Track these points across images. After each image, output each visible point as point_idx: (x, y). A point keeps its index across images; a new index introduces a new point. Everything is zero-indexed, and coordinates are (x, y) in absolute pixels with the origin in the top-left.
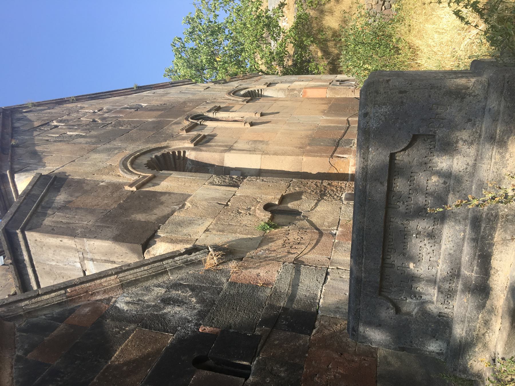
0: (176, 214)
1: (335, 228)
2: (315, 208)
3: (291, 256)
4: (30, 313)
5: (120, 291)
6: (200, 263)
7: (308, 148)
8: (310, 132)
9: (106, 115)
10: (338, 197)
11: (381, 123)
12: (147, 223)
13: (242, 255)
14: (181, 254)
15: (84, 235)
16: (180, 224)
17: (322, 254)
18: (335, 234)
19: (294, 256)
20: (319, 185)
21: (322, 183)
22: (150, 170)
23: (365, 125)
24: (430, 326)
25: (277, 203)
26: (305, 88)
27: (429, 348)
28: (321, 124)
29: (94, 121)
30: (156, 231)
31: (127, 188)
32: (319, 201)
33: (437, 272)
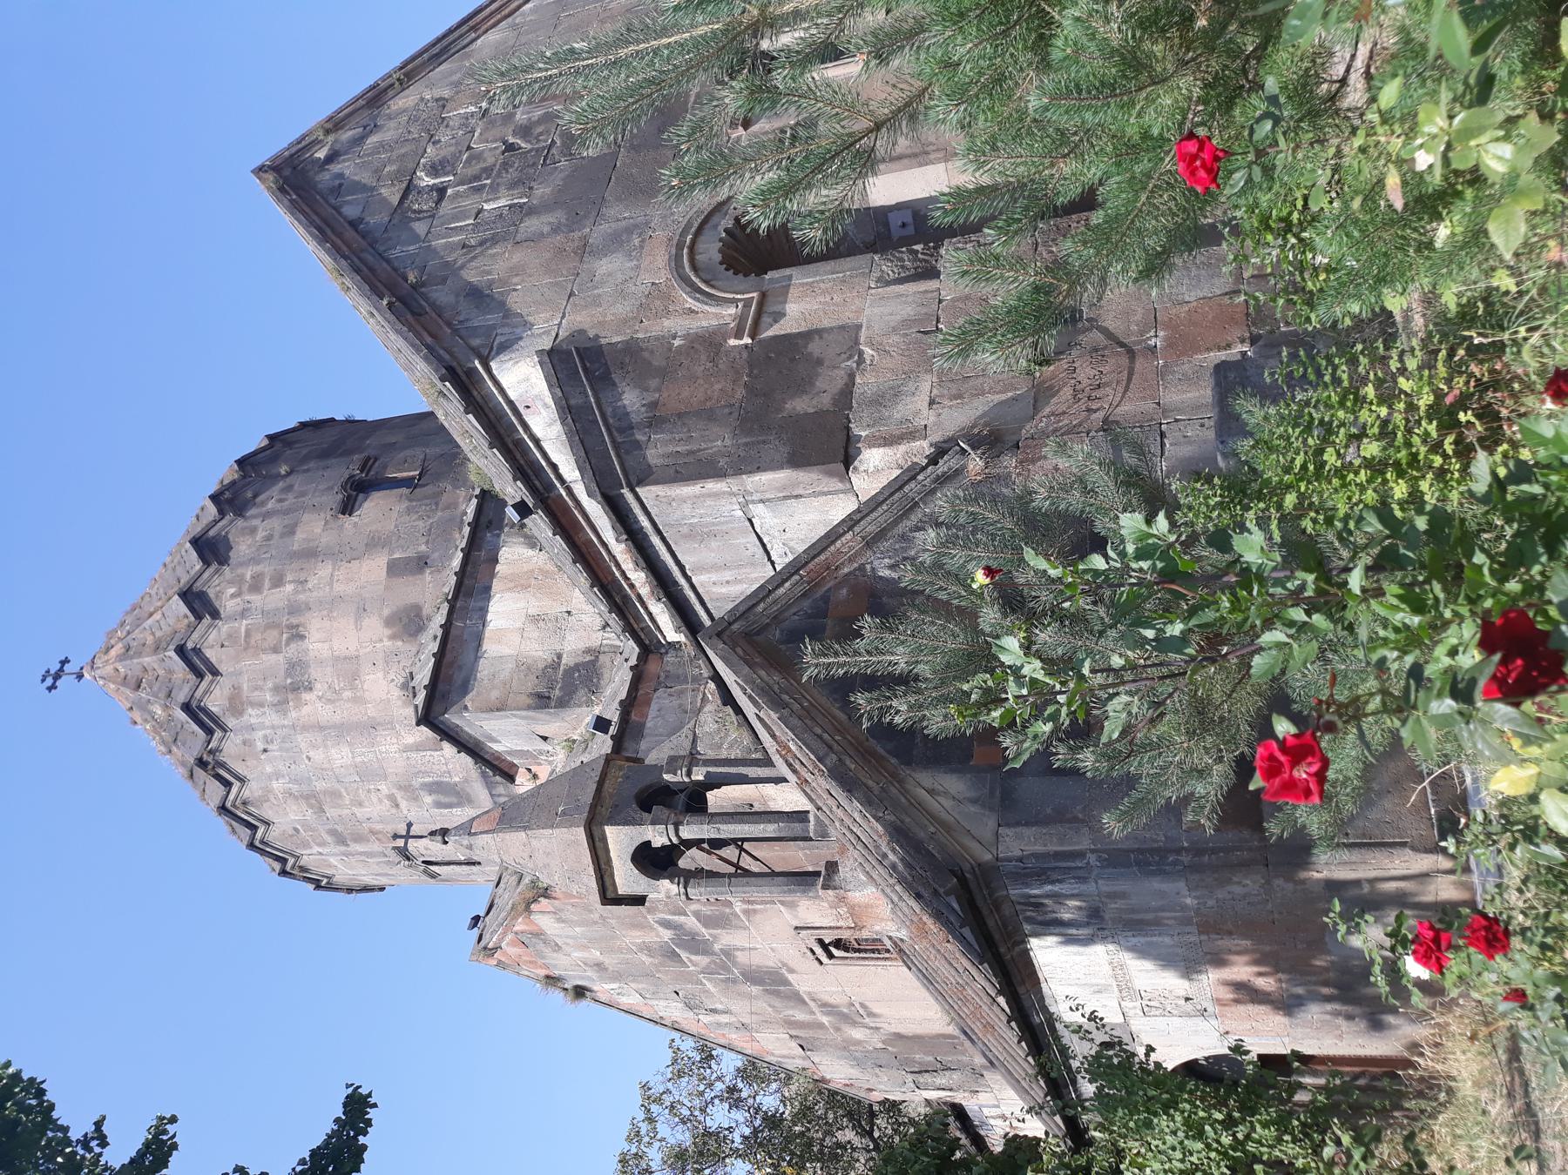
0: (858, 380)
3: (1094, 416)
4: (776, 618)
5: (869, 553)
6: (958, 472)
9: (520, 117)
12: (820, 414)
13: (1015, 438)
14: (924, 468)
15: (739, 472)
16: (879, 401)
19: (1100, 415)
22: (740, 276)
29: (510, 148)
30: (848, 429)
31: (732, 342)
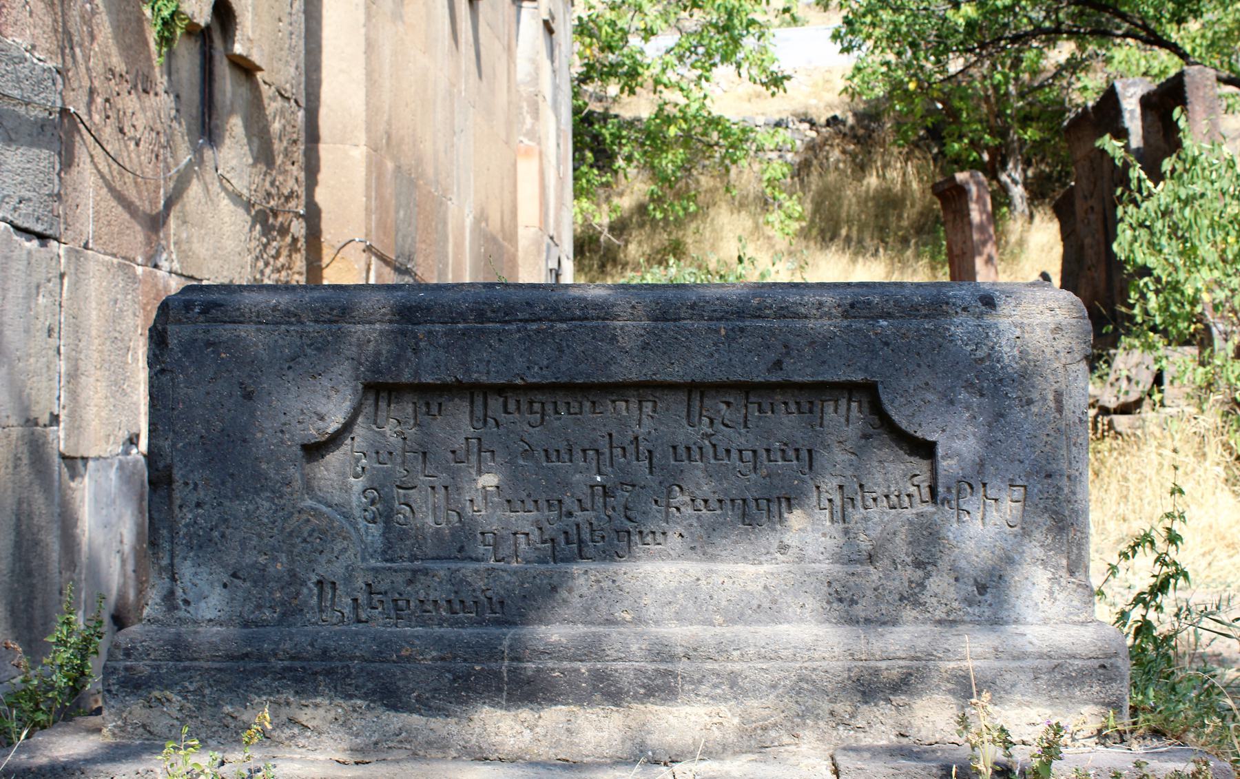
1: (176, 266)
2: (225, 189)
7: (390, 165)
8: (430, 171)
10: (262, 273)
11: (969, 348)
17: (96, 220)
18: (156, 266)
20: (292, 204)
21: (298, 216)
23: (959, 302)
24: (275, 559)
25: (238, 49)
26: (541, 154)
27: (188, 563)
28: (452, 207)
32: (248, 205)
33: (477, 560)
